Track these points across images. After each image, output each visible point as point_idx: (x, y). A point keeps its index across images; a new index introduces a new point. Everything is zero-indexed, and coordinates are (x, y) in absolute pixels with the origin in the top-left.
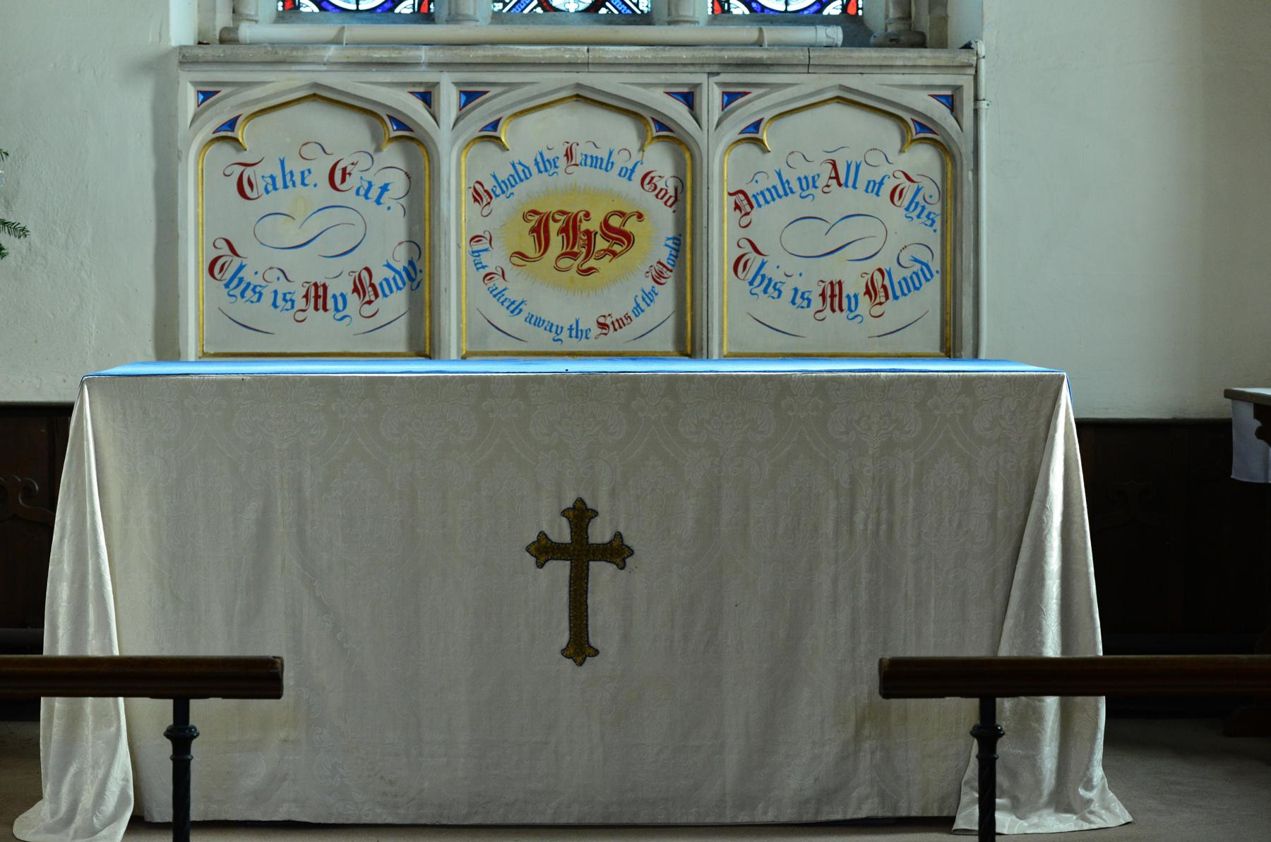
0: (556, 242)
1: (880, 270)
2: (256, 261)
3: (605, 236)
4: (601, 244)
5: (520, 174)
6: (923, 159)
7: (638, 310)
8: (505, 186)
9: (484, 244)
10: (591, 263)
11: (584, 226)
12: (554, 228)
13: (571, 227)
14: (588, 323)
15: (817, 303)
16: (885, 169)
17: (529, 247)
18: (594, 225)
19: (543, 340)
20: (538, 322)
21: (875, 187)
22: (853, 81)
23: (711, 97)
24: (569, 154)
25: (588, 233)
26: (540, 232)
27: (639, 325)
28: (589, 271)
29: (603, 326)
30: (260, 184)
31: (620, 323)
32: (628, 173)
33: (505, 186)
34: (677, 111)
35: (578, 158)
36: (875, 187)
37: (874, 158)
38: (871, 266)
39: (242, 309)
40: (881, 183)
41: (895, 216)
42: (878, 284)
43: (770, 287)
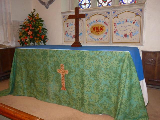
0: (95, 30)
1: (132, 32)
2: (69, 33)
3: (100, 29)
4: (100, 30)
5: (92, 23)
6: (138, 17)
7: (104, 37)
8: (90, 24)
9: (116, 31)
10: (99, 32)
11: (98, 28)
12: (95, 28)
13: (97, 28)
14: (99, 39)
15: (124, 36)
16: (133, 20)
17: (93, 30)
18: (99, 28)
19: (94, 41)
20: (94, 39)
21: (131, 22)
22: (128, 9)
23: (111, 12)
24: (97, 20)
25: (99, 29)
26: (94, 29)
27: (104, 39)
28: (99, 33)
29: (100, 39)
30: (69, 25)
31: (102, 39)
32: (103, 22)
33: (90, 24)
34: (107, 15)
35: (98, 21)
36: (131, 22)
37: (131, 18)
38: (130, 32)
39: (68, 38)
40: (132, 21)
41: (134, 26)
42: (131, 34)
43: (118, 34)
